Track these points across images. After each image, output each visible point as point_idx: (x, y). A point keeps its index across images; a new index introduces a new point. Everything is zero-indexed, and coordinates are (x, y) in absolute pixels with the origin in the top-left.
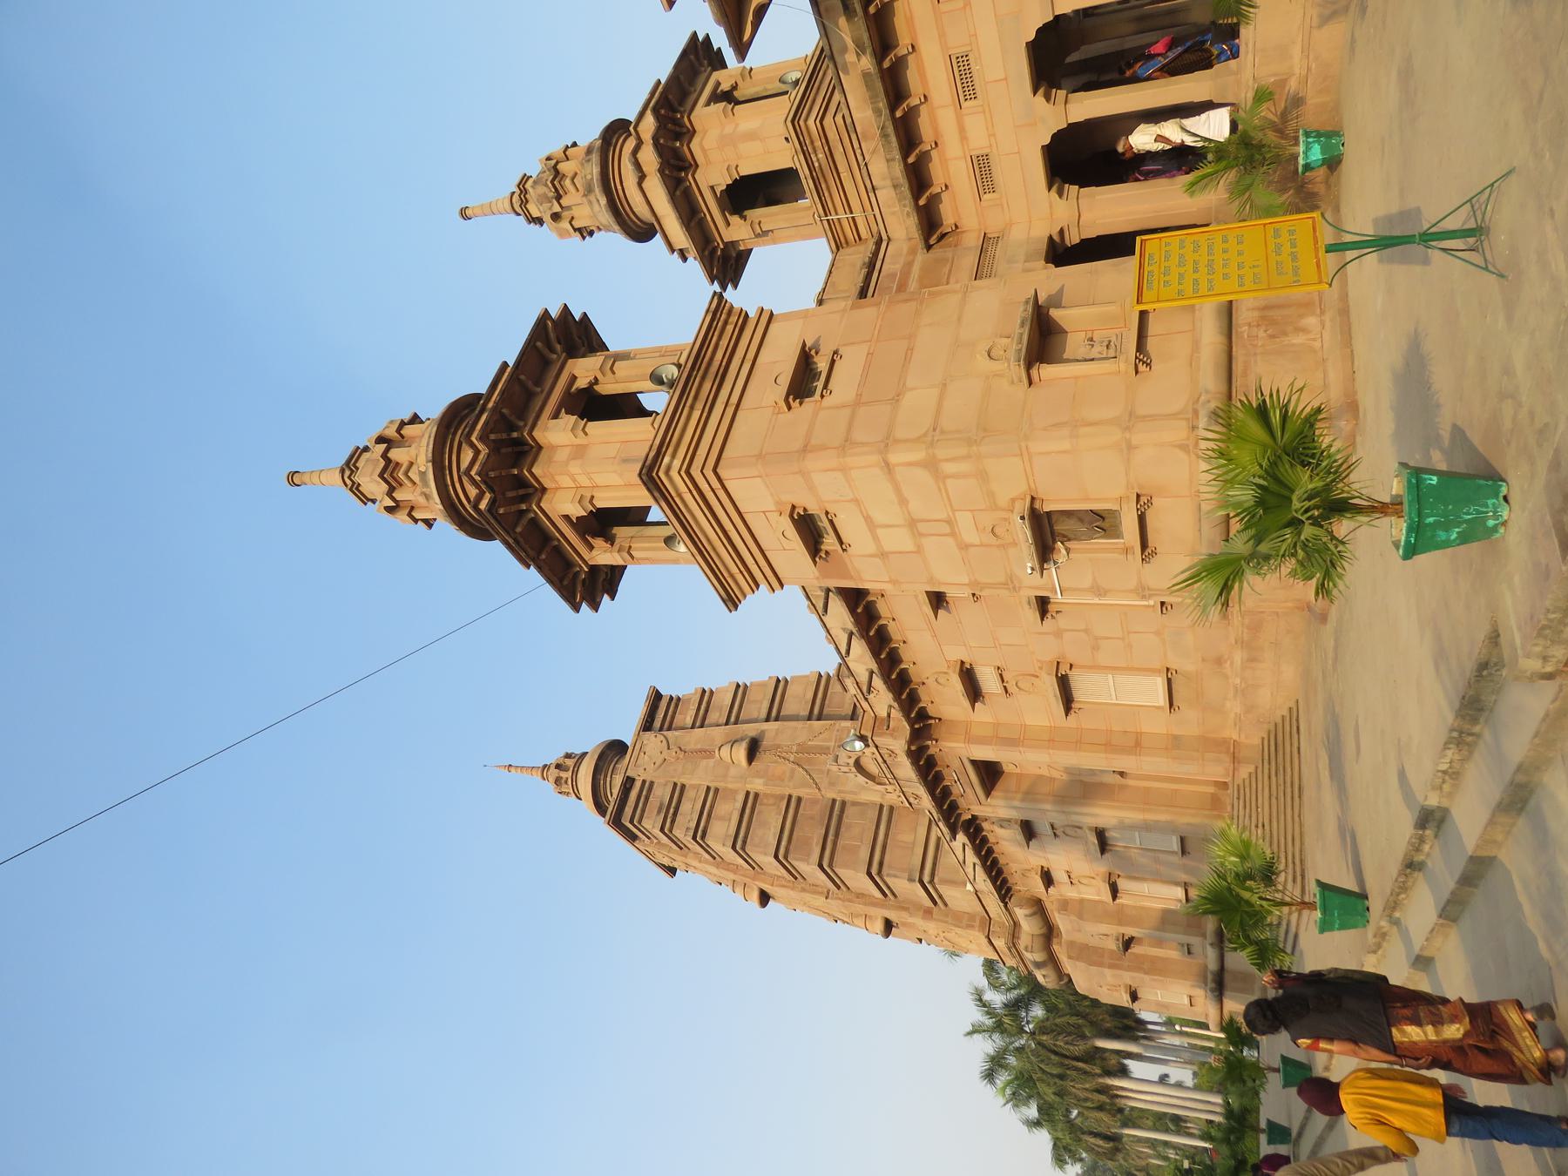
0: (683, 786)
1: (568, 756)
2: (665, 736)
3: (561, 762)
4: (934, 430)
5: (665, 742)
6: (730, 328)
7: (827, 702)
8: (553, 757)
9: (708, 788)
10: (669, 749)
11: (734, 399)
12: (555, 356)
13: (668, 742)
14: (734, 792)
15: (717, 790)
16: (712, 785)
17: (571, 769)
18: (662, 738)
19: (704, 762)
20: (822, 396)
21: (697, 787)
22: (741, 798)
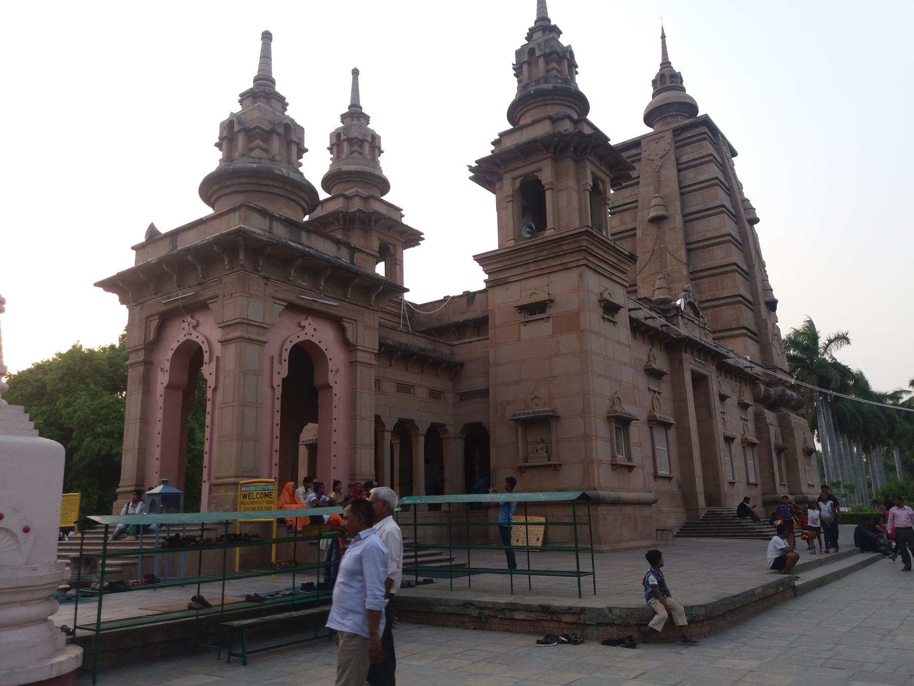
2: (669, 150)
5: (665, 152)
10: (661, 158)
12: (337, 224)
13: (664, 155)
16: (639, 204)
18: (667, 149)
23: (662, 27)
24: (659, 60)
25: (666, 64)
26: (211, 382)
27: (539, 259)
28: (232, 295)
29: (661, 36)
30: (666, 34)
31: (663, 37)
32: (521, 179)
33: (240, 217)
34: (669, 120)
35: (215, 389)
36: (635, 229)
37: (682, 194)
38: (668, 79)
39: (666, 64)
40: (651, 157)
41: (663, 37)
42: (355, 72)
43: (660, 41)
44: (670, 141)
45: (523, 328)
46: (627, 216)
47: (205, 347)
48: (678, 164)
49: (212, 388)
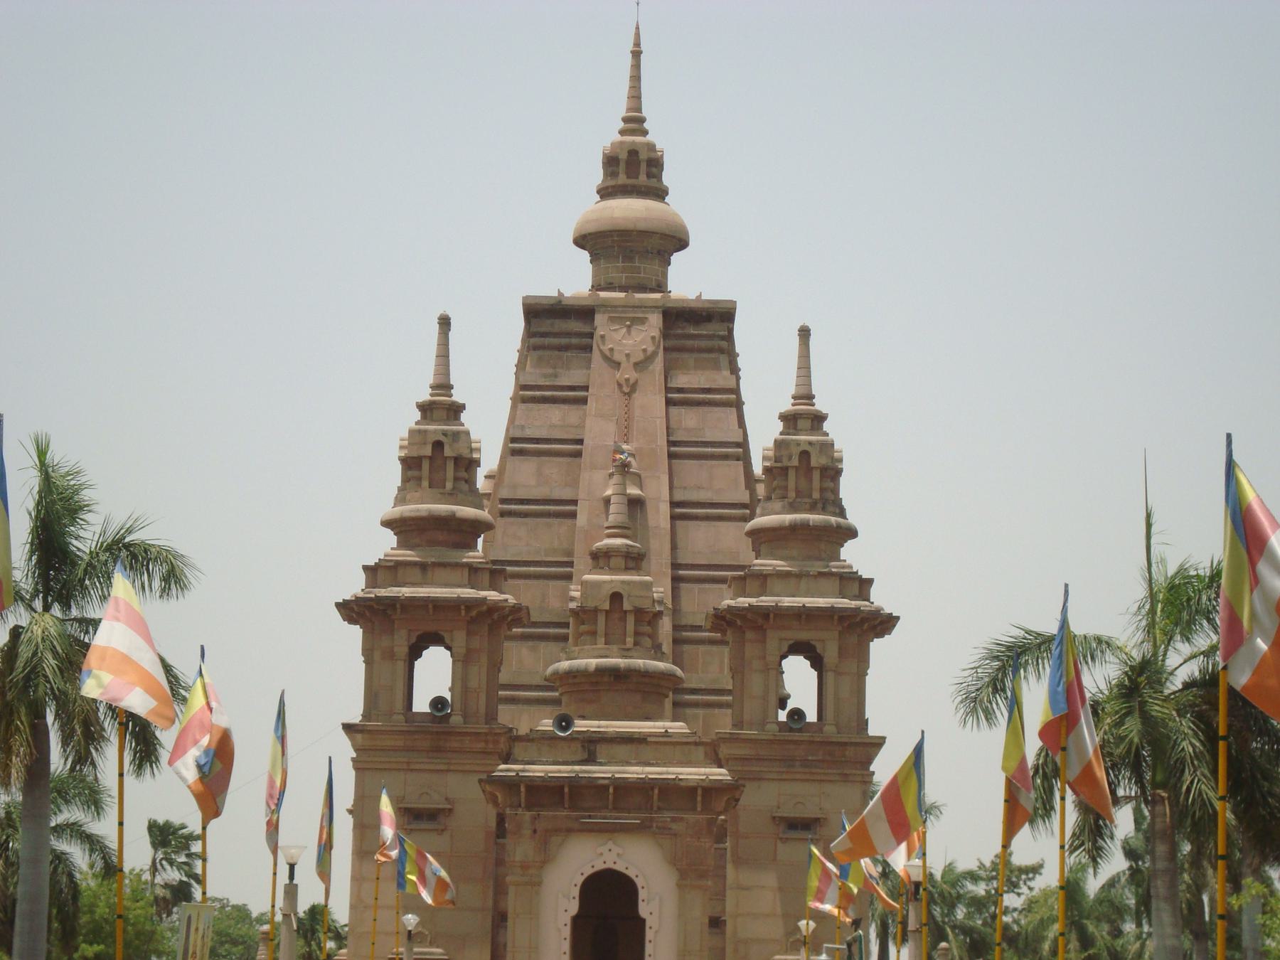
0: (584, 401)
1: (655, 164)
3: (643, 156)
4: (365, 907)
6: (482, 745)
7: (707, 586)
8: (658, 134)
9: (580, 442)
11: (412, 767)
12: (463, 613)
14: (575, 483)
15: (578, 454)
17: (630, 181)
19: (611, 428)
20: (406, 829)
21: (582, 426)
22: (566, 494)
23: (637, 28)
24: (620, 108)
25: (635, 123)
26: (651, 922)
27: (810, 758)
28: (699, 838)
29: (630, 47)
30: (643, 47)
31: (637, 54)
32: (791, 642)
33: (706, 753)
34: (637, 264)
35: (656, 932)
36: (575, 502)
37: (671, 456)
38: (643, 167)
39: (635, 123)
40: (617, 357)
41: (637, 54)
42: (445, 322)
43: (628, 60)
44: (656, 333)
45: (779, 844)
46: (554, 468)
47: (639, 882)
48: (668, 390)
49: (653, 930)
